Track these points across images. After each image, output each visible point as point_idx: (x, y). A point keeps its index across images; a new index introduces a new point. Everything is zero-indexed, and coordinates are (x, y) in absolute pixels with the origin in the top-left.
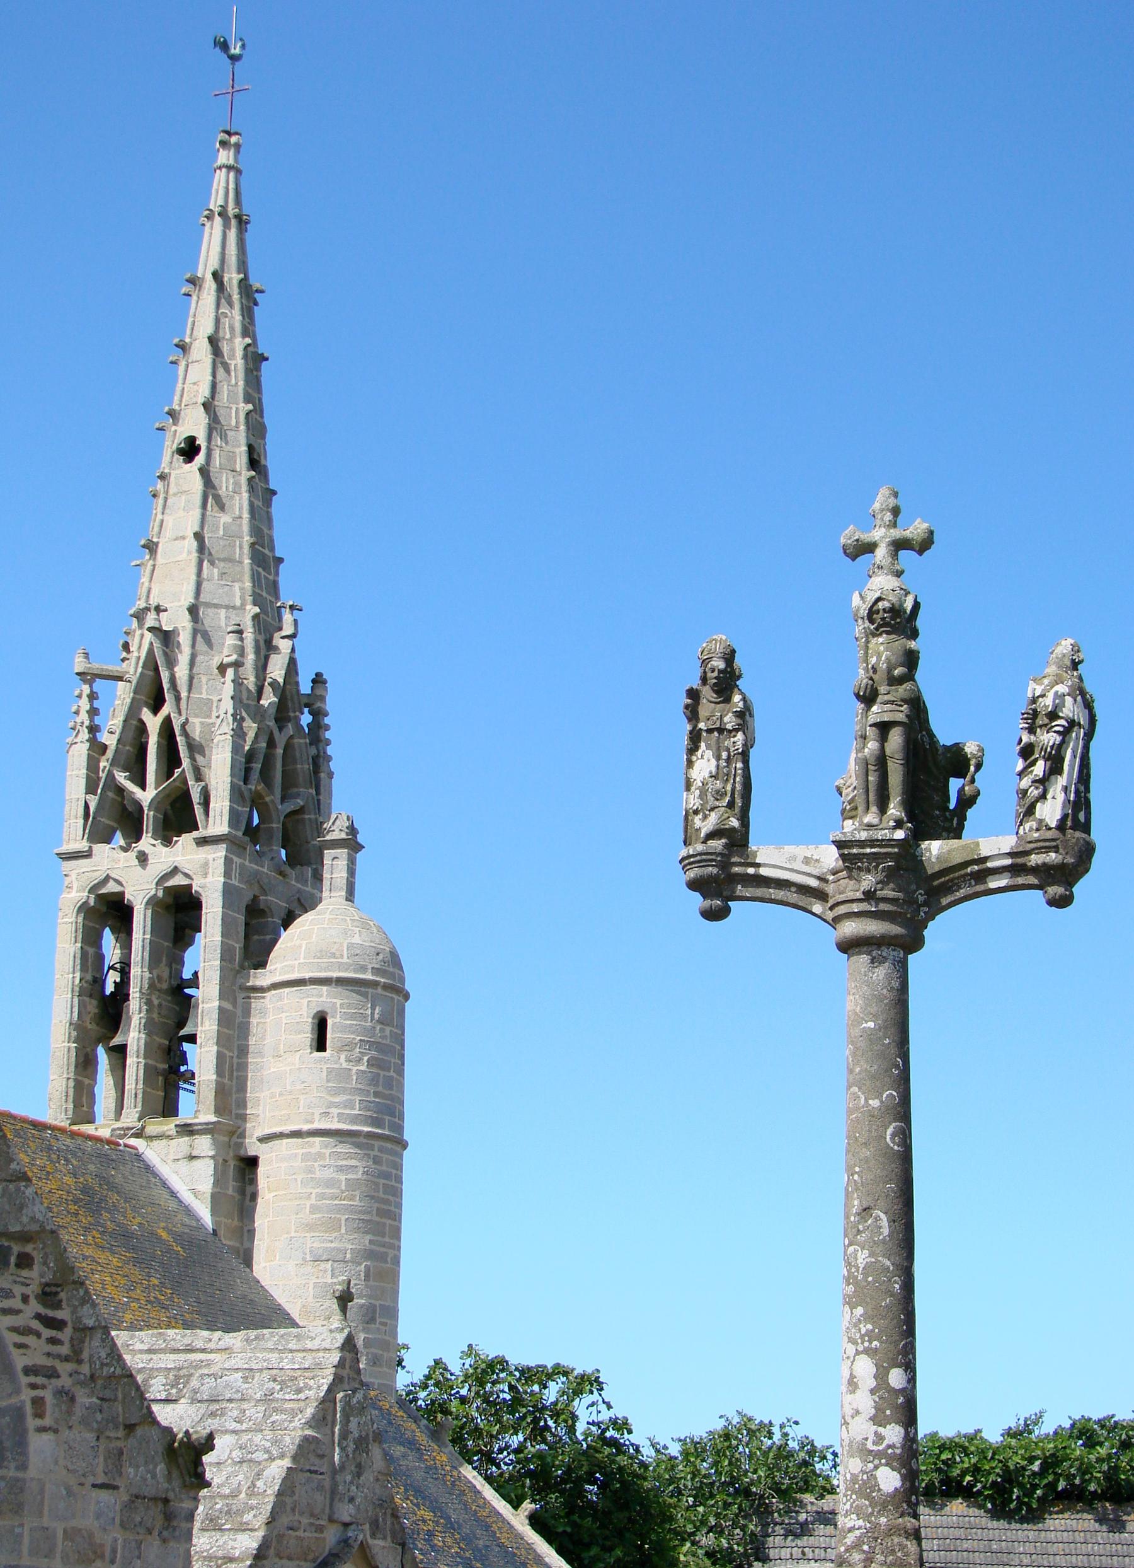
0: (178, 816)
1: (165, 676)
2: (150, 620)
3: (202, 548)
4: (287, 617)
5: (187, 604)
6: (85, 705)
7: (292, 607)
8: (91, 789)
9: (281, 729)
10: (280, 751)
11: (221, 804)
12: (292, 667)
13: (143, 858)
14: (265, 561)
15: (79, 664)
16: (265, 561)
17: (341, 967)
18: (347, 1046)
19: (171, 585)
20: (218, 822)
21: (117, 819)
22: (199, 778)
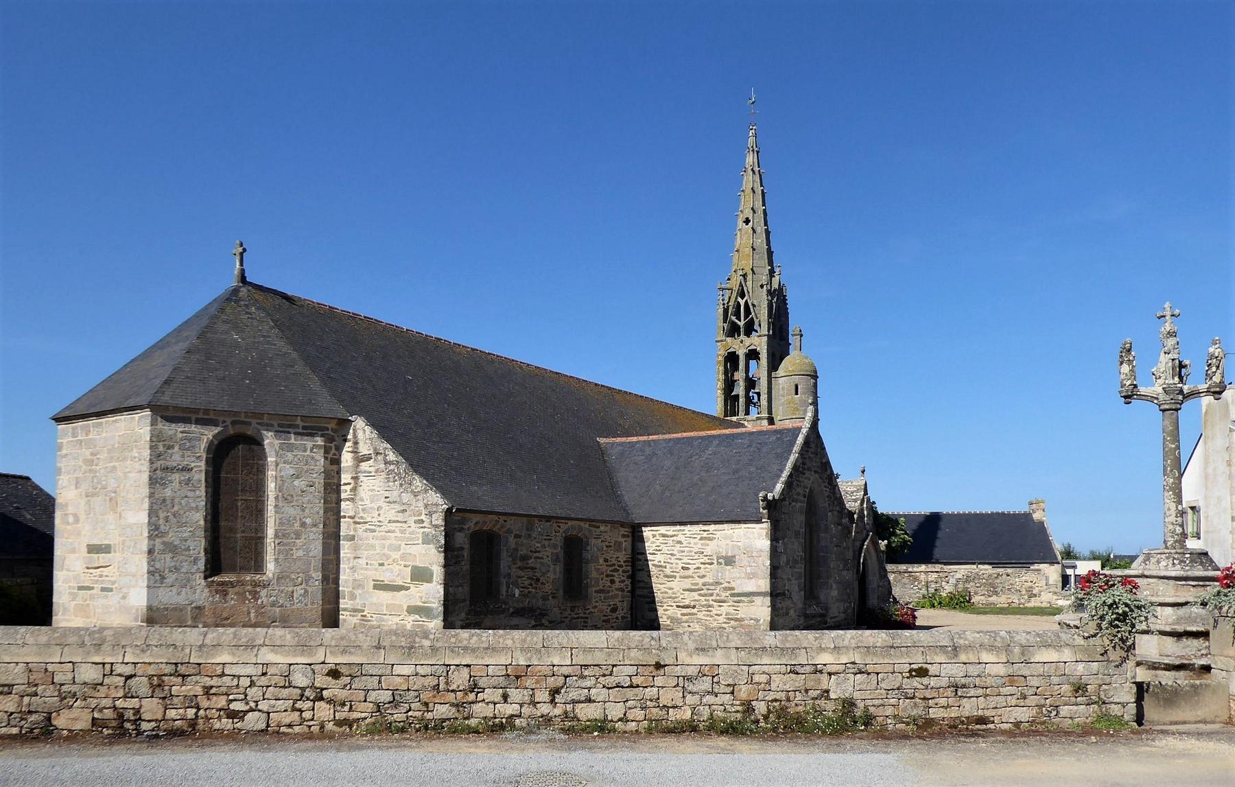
8: (725, 321)
14: (770, 253)
16: (770, 253)
21: (733, 331)
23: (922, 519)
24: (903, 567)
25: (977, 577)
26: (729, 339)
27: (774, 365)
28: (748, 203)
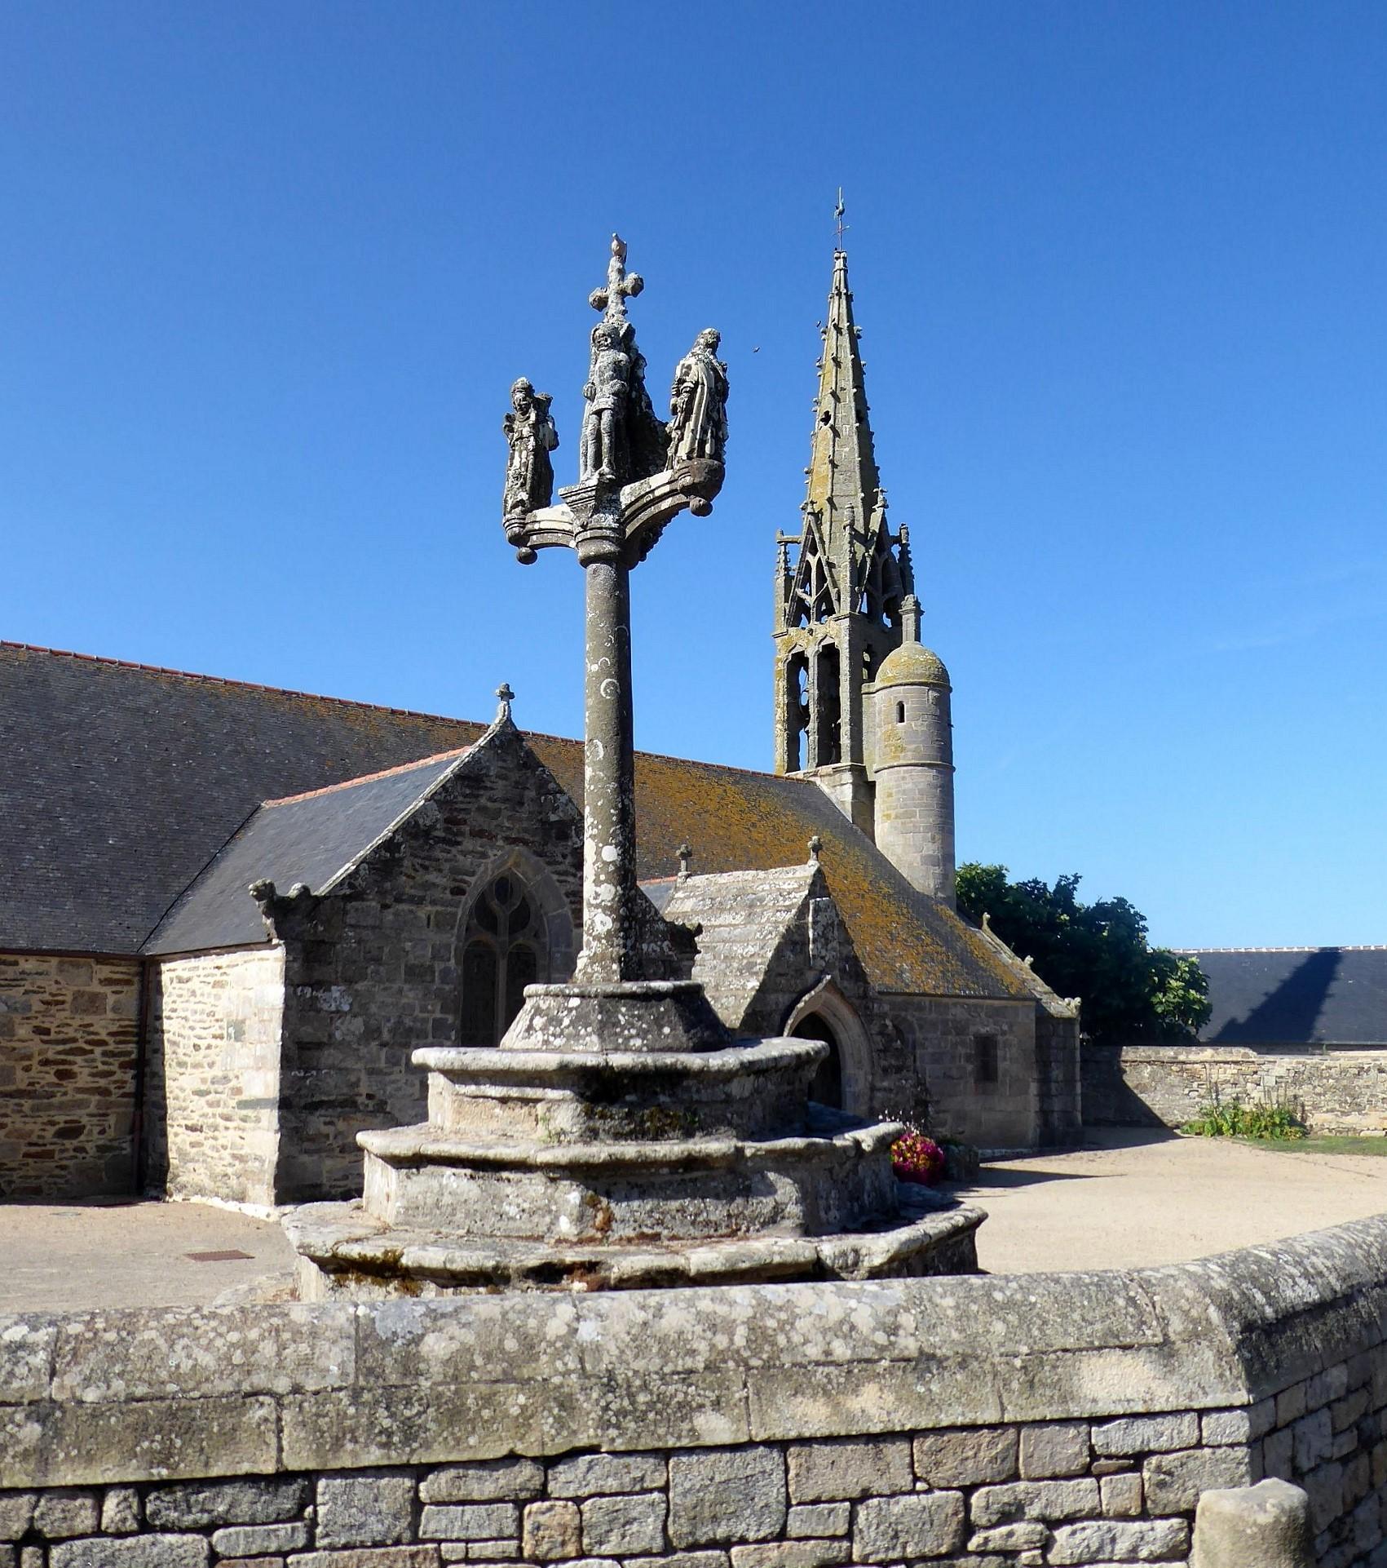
0: (826, 607)
1: (817, 536)
2: (809, 510)
3: (834, 466)
4: (880, 497)
6: (782, 557)
8: (786, 601)
11: (846, 599)
13: (811, 631)
15: (779, 537)
19: (819, 494)
20: (844, 607)
21: (798, 613)
22: (835, 585)
23: (1303, 961)
24: (1168, 1052)
25: (1318, 1074)
27: (865, 670)
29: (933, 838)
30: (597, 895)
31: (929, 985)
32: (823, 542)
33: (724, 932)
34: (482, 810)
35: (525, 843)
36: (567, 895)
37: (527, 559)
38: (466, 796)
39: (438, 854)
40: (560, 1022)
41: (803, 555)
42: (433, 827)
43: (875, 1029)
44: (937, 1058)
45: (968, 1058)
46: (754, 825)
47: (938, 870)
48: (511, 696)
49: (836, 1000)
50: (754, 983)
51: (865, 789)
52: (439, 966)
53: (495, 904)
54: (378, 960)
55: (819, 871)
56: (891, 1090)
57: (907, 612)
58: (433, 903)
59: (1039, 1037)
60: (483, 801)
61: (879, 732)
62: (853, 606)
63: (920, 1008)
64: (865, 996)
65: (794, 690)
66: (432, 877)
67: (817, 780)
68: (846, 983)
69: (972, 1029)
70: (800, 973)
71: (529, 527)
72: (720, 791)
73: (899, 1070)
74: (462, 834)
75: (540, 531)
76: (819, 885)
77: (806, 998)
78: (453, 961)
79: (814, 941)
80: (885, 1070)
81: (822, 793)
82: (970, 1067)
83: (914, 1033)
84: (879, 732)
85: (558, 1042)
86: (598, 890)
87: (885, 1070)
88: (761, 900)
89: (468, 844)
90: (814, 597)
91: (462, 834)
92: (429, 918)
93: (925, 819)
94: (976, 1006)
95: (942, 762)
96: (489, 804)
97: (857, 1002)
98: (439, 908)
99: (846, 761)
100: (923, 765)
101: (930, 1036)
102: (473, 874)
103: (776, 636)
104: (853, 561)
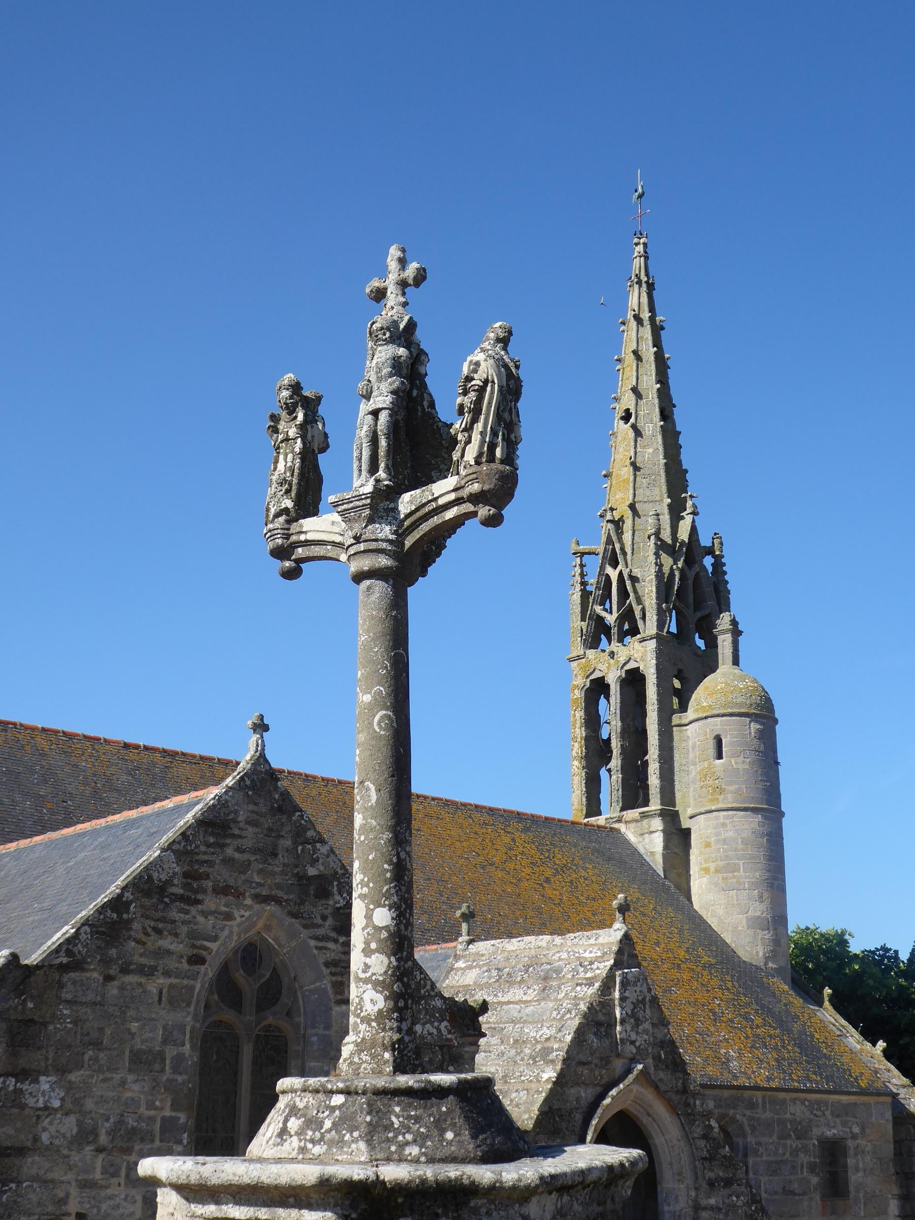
0: (629, 627)
1: (617, 546)
2: (609, 517)
3: (636, 468)
4: (689, 503)
5: (628, 503)
6: (578, 570)
7: (691, 497)
8: (583, 620)
9: (690, 569)
10: (690, 582)
12: (694, 530)
13: (612, 655)
15: (574, 548)
17: (724, 707)
18: (735, 755)
20: (650, 627)
21: (597, 634)
22: (639, 601)
26: (591, 653)
27: (677, 697)
28: (635, 376)
29: (761, 897)
30: (367, 967)
31: (761, 1076)
32: (624, 553)
33: (514, 1010)
34: (228, 862)
35: (278, 901)
36: (327, 964)
37: (292, 574)
38: (209, 845)
39: (174, 914)
40: (321, 1124)
41: (602, 568)
42: (169, 882)
43: (698, 1131)
44: (774, 1169)
45: (812, 1168)
46: (547, 880)
47: (768, 935)
48: (266, 728)
49: (649, 1096)
50: (550, 1074)
51: (678, 838)
52: (170, 1052)
53: (240, 977)
54: (97, 1045)
55: (626, 937)
56: (719, 1209)
57: (724, 632)
58: (167, 974)
59: (898, 1142)
60: (229, 851)
61: (694, 771)
62: (661, 624)
63: (752, 1105)
64: (685, 1090)
65: (592, 721)
66: (166, 943)
67: (622, 827)
68: (662, 1075)
69: (816, 1132)
70: (606, 1061)
71: (294, 538)
72: (507, 839)
73: (728, 1183)
74: (204, 891)
75: (307, 543)
76: (626, 954)
77: (614, 1092)
78: (188, 1046)
79: (623, 1022)
80: (711, 1184)
81: (627, 842)
82: (815, 1180)
83: (745, 1136)
84: (694, 771)
85: (317, 1150)
86: (368, 960)
87: (711, 1184)
88: (558, 971)
89: (210, 902)
90: (615, 615)
91: (204, 891)
92: (161, 993)
93: (749, 874)
94: (819, 1103)
95: (768, 805)
96: (237, 855)
97: (675, 1098)
98: (173, 981)
99: (655, 805)
100: (745, 809)
101: (765, 1140)
102: (215, 939)
103: (571, 660)
104: (659, 574)
